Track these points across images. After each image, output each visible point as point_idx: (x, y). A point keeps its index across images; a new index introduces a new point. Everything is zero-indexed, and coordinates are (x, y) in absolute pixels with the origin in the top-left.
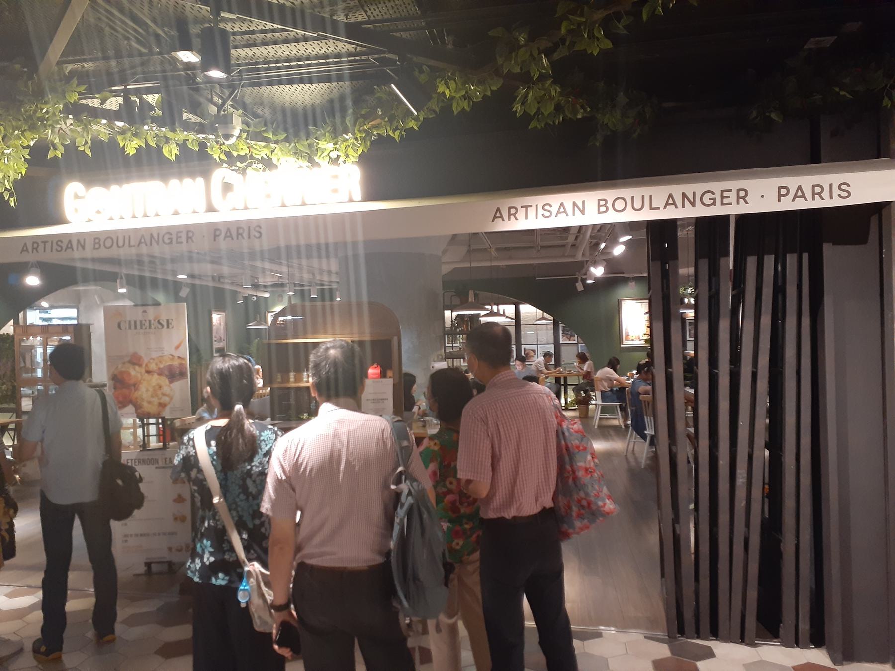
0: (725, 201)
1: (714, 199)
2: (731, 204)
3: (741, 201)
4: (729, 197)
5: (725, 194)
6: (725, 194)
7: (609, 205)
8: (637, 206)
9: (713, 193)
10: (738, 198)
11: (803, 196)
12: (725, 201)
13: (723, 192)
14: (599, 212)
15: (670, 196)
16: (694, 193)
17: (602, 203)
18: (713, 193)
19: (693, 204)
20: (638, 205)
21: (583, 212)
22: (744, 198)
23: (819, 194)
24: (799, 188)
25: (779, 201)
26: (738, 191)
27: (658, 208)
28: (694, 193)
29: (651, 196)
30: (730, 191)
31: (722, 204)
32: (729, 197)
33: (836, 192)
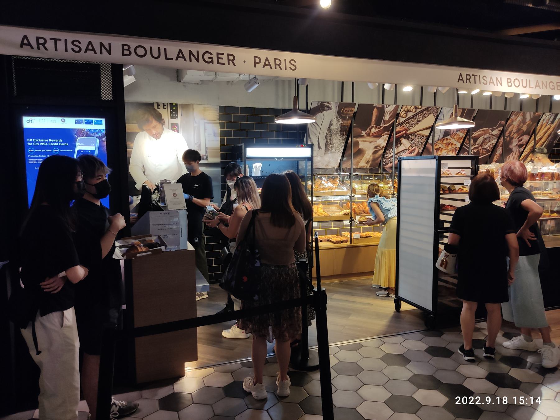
0: (220, 61)
1: (212, 58)
2: (223, 64)
3: (231, 62)
4: (222, 59)
5: (220, 56)
6: (220, 56)
7: (132, 50)
8: (156, 54)
9: (211, 54)
10: (229, 60)
11: (93, 49)
12: (220, 61)
13: (218, 54)
14: (123, 54)
15: (180, 51)
16: (198, 52)
17: (126, 47)
18: (211, 54)
19: (198, 60)
20: (156, 54)
21: (109, 52)
22: (232, 61)
23: (279, 65)
24: (267, 59)
25: (255, 67)
26: (229, 55)
27: (172, 59)
28: (198, 52)
29: (165, 49)
30: (223, 54)
31: (218, 63)
32: (222, 59)
33: (70, 46)
